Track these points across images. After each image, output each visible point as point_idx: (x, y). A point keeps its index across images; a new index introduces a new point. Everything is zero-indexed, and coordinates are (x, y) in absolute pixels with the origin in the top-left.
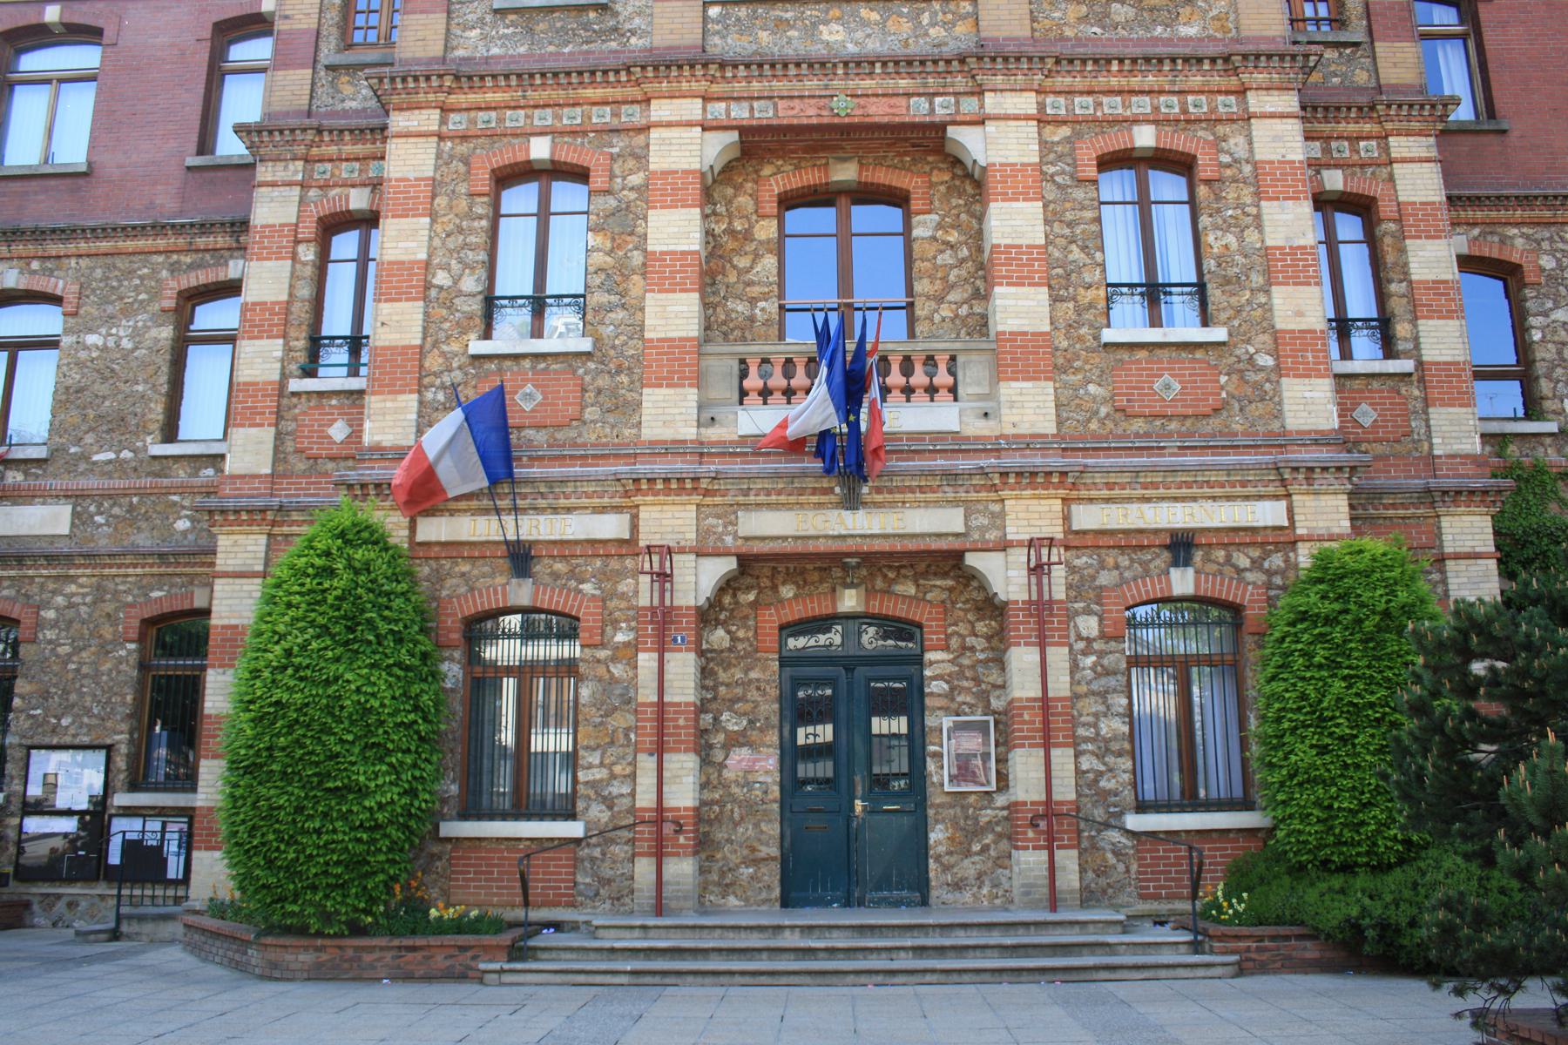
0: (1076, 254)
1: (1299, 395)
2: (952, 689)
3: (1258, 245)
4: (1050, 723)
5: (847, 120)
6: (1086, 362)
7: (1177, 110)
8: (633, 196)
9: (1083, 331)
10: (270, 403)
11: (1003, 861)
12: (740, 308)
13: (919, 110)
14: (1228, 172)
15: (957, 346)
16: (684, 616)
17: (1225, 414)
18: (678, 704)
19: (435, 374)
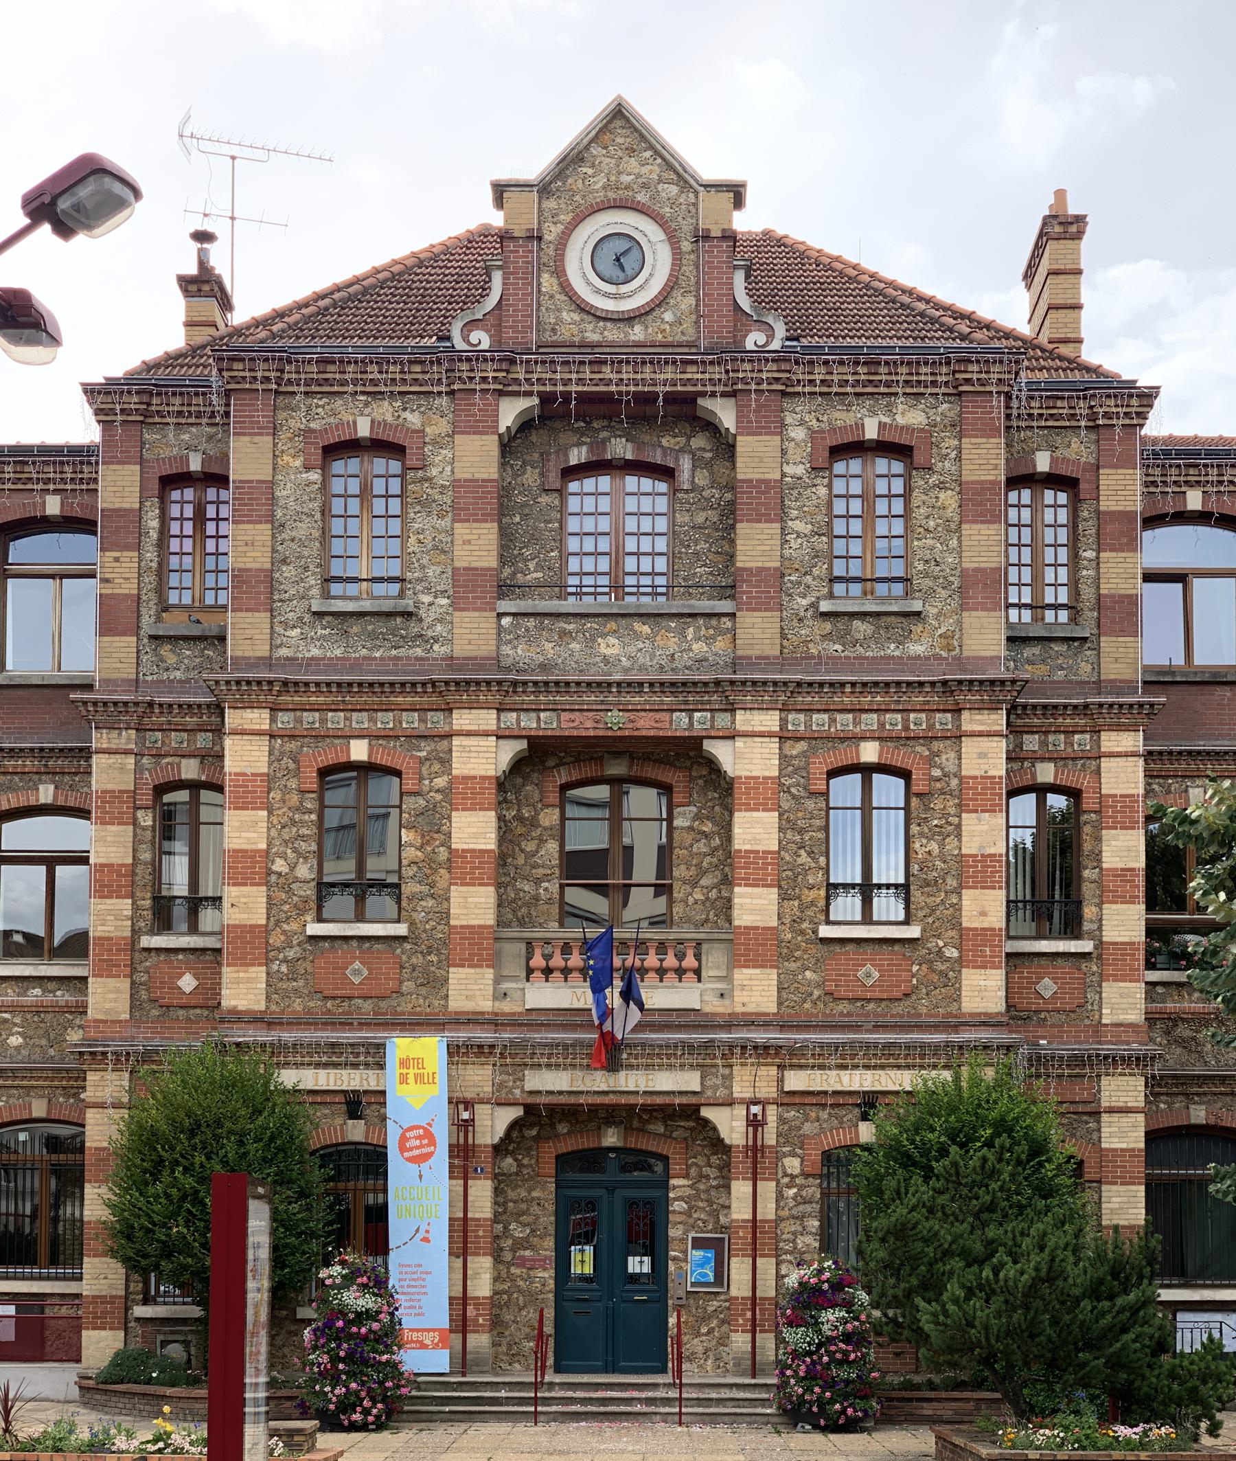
0: (804, 858)
1: (975, 983)
2: (690, 1208)
3: (956, 852)
4: (759, 1238)
5: (619, 733)
6: (805, 951)
7: (900, 727)
8: (439, 797)
9: (805, 925)
10: (124, 957)
11: (723, 1341)
12: (526, 888)
13: (679, 724)
14: (938, 785)
15: (702, 936)
16: (483, 1152)
17: (914, 997)
18: (479, 1220)
19: (279, 950)
